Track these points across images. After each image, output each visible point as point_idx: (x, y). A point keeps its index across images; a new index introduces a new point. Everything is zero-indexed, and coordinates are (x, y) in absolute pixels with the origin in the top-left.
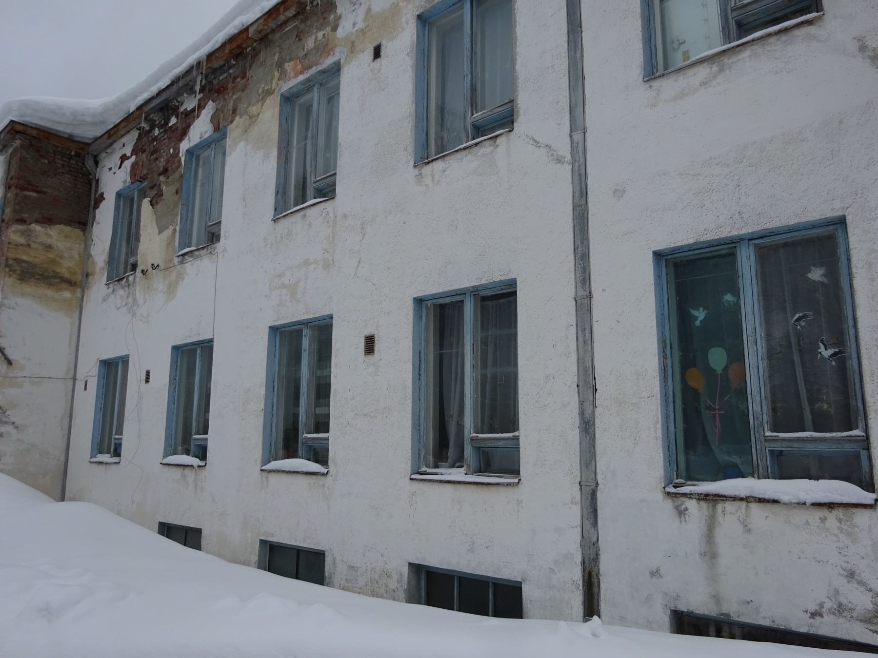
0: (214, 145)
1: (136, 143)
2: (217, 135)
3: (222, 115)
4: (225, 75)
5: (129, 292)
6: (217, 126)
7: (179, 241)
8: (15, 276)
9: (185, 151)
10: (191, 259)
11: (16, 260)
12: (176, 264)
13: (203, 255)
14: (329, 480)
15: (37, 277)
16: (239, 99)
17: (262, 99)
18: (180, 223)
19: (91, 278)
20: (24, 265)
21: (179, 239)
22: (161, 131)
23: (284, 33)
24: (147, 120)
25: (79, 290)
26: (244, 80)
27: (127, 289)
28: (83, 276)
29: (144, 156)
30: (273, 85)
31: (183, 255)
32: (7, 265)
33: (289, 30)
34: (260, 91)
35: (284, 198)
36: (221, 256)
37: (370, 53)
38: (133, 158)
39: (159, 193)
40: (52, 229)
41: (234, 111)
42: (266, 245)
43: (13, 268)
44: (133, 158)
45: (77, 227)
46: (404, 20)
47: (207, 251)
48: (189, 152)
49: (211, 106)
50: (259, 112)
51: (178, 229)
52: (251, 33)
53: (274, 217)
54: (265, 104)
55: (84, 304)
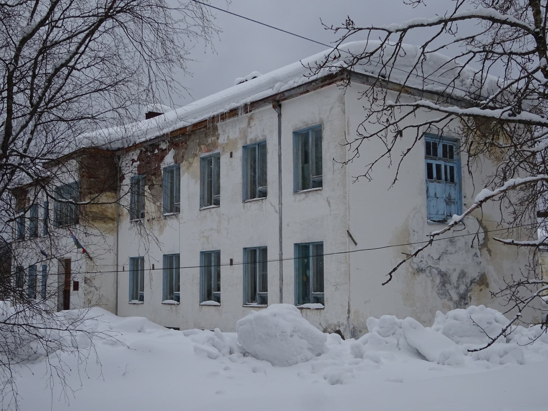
2: (176, 165)
4: (178, 139)
14: (221, 307)
16: (183, 152)
19: (121, 217)
20: (93, 214)
26: (186, 145)
37: (228, 155)
38: (138, 163)
41: (183, 157)
44: (138, 163)
46: (239, 146)
51: (162, 203)
55: (119, 229)
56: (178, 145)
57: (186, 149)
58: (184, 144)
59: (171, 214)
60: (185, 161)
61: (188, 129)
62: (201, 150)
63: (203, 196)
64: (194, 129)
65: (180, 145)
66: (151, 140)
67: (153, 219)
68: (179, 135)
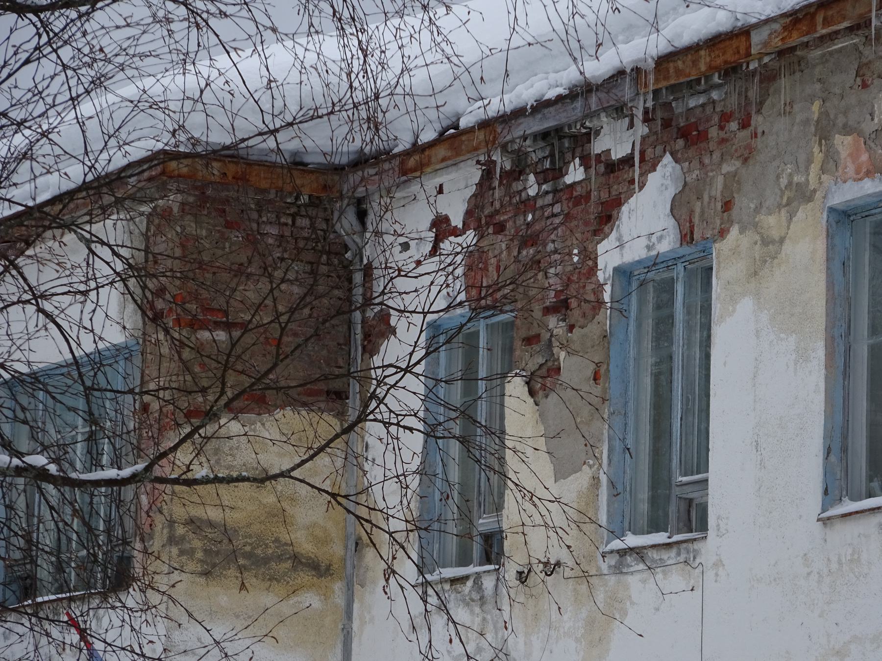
0: (680, 267)
1: (474, 195)
2: (686, 250)
3: (699, 204)
4: (702, 100)
5: (484, 619)
6: (686, 229)
7: (608, 511)
8: (191, 566)
9: (610, 271)
10: (641, 566)
11: (191, 522)
12: (606, 572)
13: (669, 562)
15: (241, 561)
16: (733, 177)
17: (787, 204)
18: (609, 464)
21: (608, 506)
22: (544, 187)
23: (831, 53)
24: (508, 152)
25: (338, 587)
27: (477, 610)
28: (346, 547)
29: (501, 243)
30: (810, 178)
31: (623, 553)
32: (172, 540)
33: (840, 50)
34: (784, 181)
35: (844, 461)
36: (710, 575)
39: (550, 364)
40: (268, 424)
41: (727, 206)
42: (809, 574)
43: (187, 546)
45: (322, 405)
47: (679, 554)
48: (623, 273)
49: (669, 169)
50: (783, 235)
52: (757, 45)
53: (823, 511)
54: (794, 219)
55: (355, 625)
56: (703, 136)
57: (746, 160)
58: (733, 126)
59: (660, 538)
60: (742, 231)
61: (757, 38)
62: (831, 162)
63: (845, 437)
64: (795, 39)
65: (713, 132)
66: (542, 106)
67: (551, 568)
68: (708, 78)
